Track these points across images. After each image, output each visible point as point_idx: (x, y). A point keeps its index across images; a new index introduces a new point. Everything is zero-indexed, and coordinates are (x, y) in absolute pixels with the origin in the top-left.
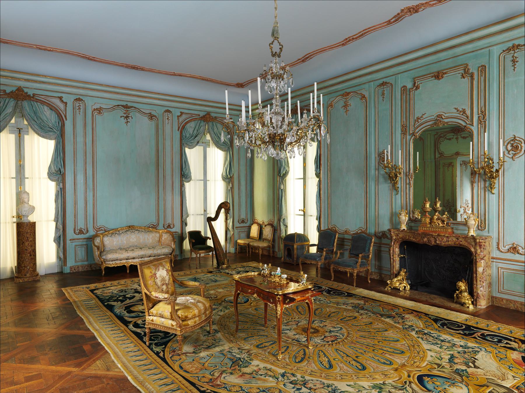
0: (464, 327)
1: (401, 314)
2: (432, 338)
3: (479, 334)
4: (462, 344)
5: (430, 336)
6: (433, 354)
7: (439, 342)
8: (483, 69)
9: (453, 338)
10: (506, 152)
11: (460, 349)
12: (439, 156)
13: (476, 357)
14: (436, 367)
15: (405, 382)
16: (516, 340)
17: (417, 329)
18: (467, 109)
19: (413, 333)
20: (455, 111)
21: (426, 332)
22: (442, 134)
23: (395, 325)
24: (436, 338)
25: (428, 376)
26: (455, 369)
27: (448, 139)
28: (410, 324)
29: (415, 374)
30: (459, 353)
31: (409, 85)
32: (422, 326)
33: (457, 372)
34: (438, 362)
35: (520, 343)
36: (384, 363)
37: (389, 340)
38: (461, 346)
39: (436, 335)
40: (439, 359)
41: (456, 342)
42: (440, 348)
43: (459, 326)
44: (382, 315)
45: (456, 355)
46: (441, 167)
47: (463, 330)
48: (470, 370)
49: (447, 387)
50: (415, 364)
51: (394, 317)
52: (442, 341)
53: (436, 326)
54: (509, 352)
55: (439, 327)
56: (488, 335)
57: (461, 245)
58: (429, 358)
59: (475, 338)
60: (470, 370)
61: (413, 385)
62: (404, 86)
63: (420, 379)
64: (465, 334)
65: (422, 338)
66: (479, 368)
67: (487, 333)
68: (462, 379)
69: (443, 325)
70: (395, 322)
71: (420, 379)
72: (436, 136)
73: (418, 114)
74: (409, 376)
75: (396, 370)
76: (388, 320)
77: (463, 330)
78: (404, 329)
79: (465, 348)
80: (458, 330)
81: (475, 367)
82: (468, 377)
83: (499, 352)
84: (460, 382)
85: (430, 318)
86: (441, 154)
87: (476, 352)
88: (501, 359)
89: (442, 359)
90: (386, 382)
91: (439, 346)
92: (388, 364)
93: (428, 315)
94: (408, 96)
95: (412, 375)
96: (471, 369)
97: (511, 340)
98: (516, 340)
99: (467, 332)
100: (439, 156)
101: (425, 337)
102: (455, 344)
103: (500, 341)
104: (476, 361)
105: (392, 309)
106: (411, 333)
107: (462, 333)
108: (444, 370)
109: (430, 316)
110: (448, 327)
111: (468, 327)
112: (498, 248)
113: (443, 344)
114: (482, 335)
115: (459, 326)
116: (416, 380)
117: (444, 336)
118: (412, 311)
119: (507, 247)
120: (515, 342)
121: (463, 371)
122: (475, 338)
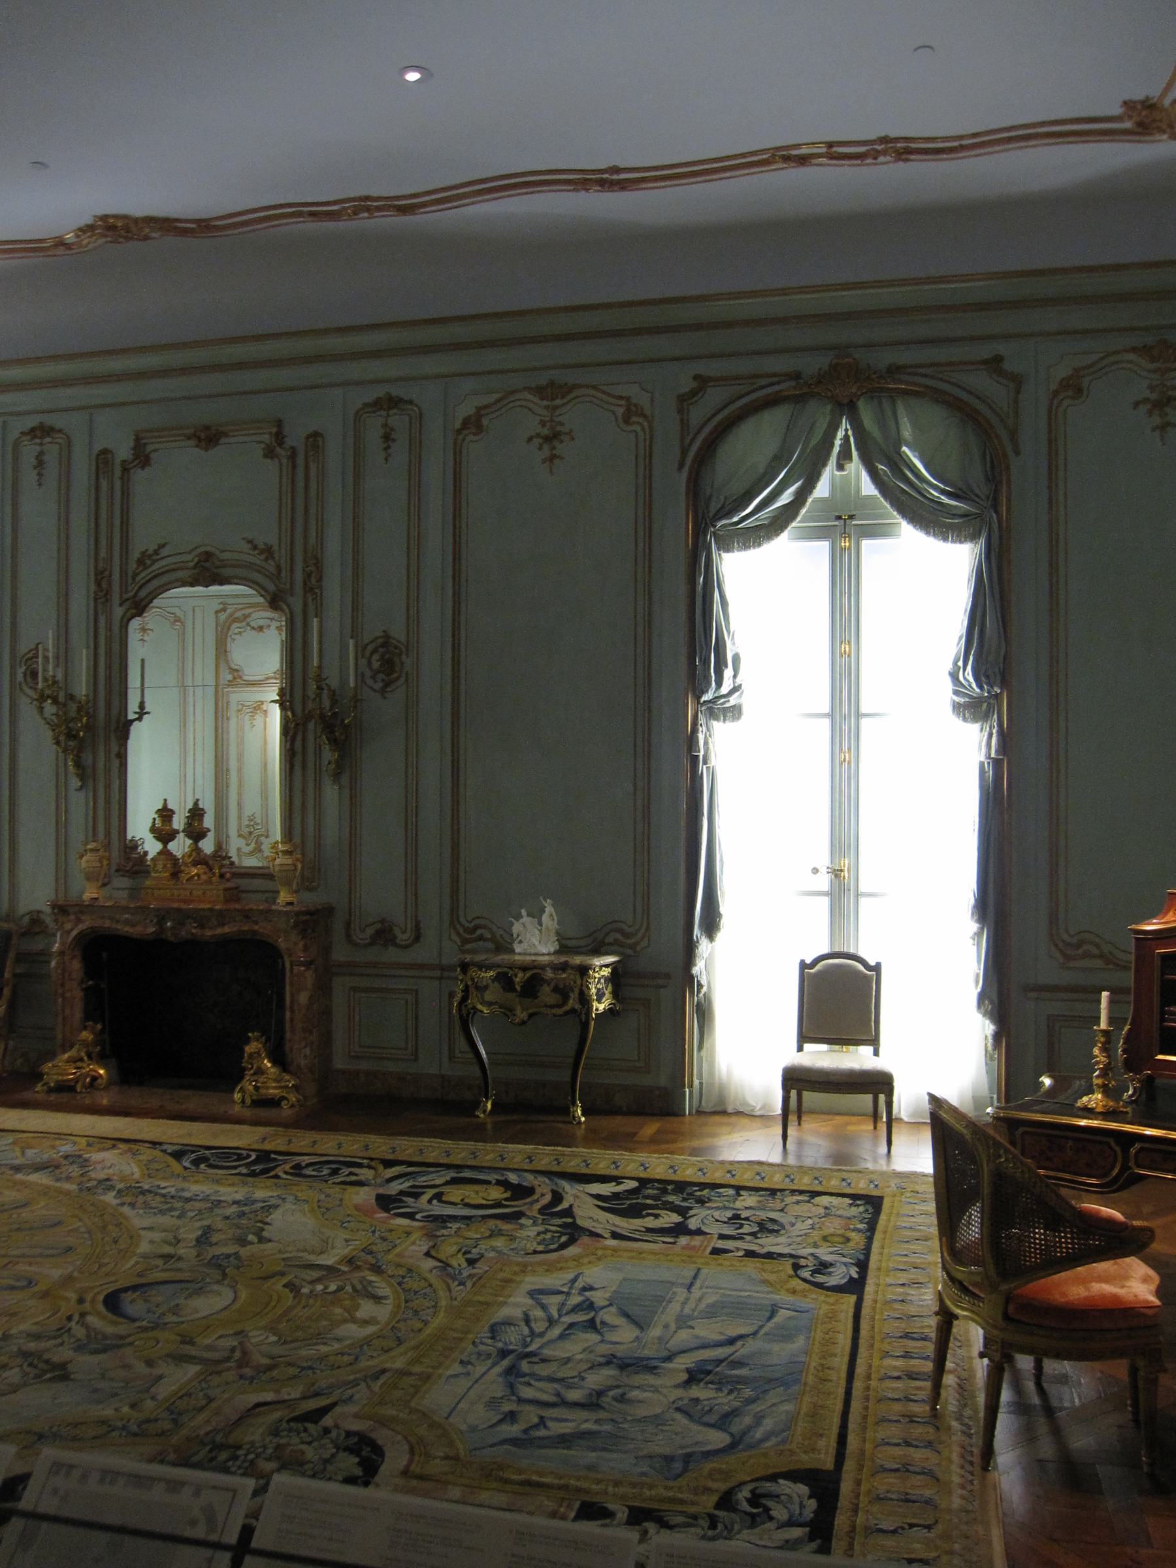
0: (254, 1157)
1: (80, 1156)
2: (158, 1199)
3: (287, 1167)
4: (238, 1197)
5: (156, 1194)
6: (157, 1236)
7: (179, 1205)
8: (315, 439)
9: (217, 1188)
10: (368, 673)
11: (234, 1209)
12: (230, 677)
13: (268, 1220)
14: (160, 1262)
15: (69, 1318)
16: (373, 1164)
17: (121, 1186)
18: (276, 548)
19: (110, 1198)
20: (246, 547)
21: (146, 1187)
22: (237, 610)
23: (58, 1184)
24: (172, 1197)
25: (134, 1288)
26: (209, 1257)
27: (253, 628)
28: (102, 1175)
29: (98, 1293)
30: (227, 1218)
31: (124, 452)
32: (137, 1176)
33: (217, 1264)
34: (168, 1250)
35: (381, 1167)
36: (12, 1288)
37: (31, 1229)
38: (235, 1202)
39: (172, 1190)
40: (170, 1244)
41: (224, 1195)
42: (179, 1217)
43: (240, 1157)
44: (17, 1169)
45: (219, 1224)
46: (232, 713)
47: (248, 1165)
48: (244, 1252)
49: (182, 1301)
50: (104, 1269)
51: (57, 1167)
52: (188, 1200)
53: (175, 1166)
54: (351, 1189)
55: (186, 1168)
56: (308, 1165)
57: (255, 933)
58: (144, 1247)
59: (277, 1177)
60: (244, 1252)
61: (90, 1319)
62: (105, 452)
63: (113, 1302)
64: (253, 1174)
65: (132, 1205)
66: (270, 1241)
67: (307, 1159)
68: (225, 1275)
69: (196, 1162)
70: (58, 1180)
71: (113, 1302)
72: (223, 616)
73: (142, 542)
74: (81, 1301)
75: (45, 1295)
76: (35, 1178)
77: (248, 1165)
78: (81, 1190)
79: (245, 1205)
80: (235, 1167)
81: (262, 1240)
82: (238, 1268)
83: (328, 1196)
84: (218, 1282)
85: (164, 1151)
86: (236, 672)
87: (270, 1208)
88: (328, 1209)
89: (179, 1241)
90: (14, 1331)
91: (176, 1213)
92: (23, 1288)
93: (160, 1144)
94: (118, 484)
95: (89, 1298)
96: (249, 1247)
97: (360, 1166)
98: (373, 1164)
99: (258, 1168)
100: (230, 677)
101: (141, 1199)
102: (220, 1201)
103: (335, 1172)
104: (266, 1227)
105: (53, 1147)
106: (102, 1198)
107: (244, 1170)
108: (180, 1265)
109: (165, 1147)
110: (211, 1166)
111: (264, 1156)
112: (348, 936)
113: (188, 1206)
114: (298, 1167)
115: (240, 1157)
116: (101, 1307)
117: (195, 1188)
118: (116, 1141)
119: (370, 931)
120: (369, 1167)
121: (228, 1256)
122: (277, 1177)
